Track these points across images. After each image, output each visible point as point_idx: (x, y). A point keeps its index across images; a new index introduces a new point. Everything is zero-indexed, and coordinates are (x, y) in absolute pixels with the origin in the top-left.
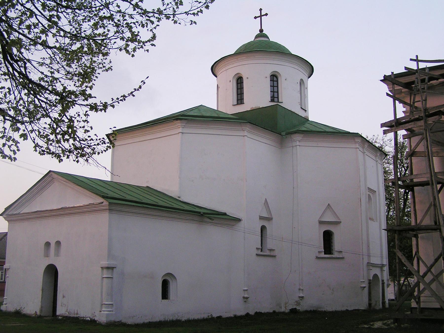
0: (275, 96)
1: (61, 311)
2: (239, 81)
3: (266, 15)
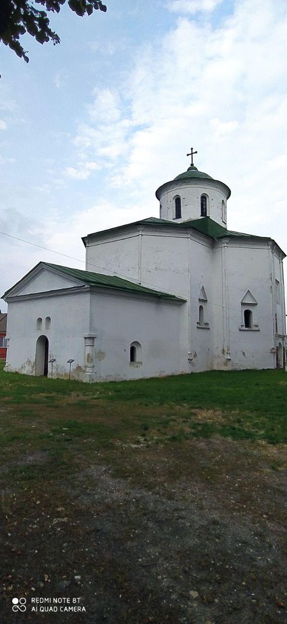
0: (204, 212)
1: (53, 371)
3: (196, 152)
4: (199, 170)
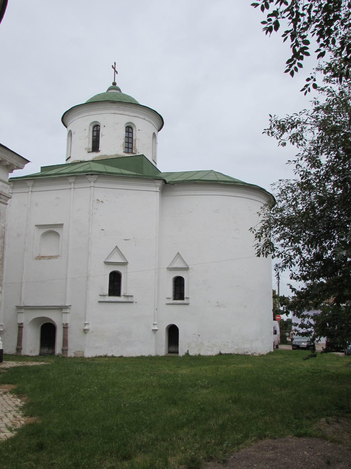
2: (95, 129)
4: (123, 91)
